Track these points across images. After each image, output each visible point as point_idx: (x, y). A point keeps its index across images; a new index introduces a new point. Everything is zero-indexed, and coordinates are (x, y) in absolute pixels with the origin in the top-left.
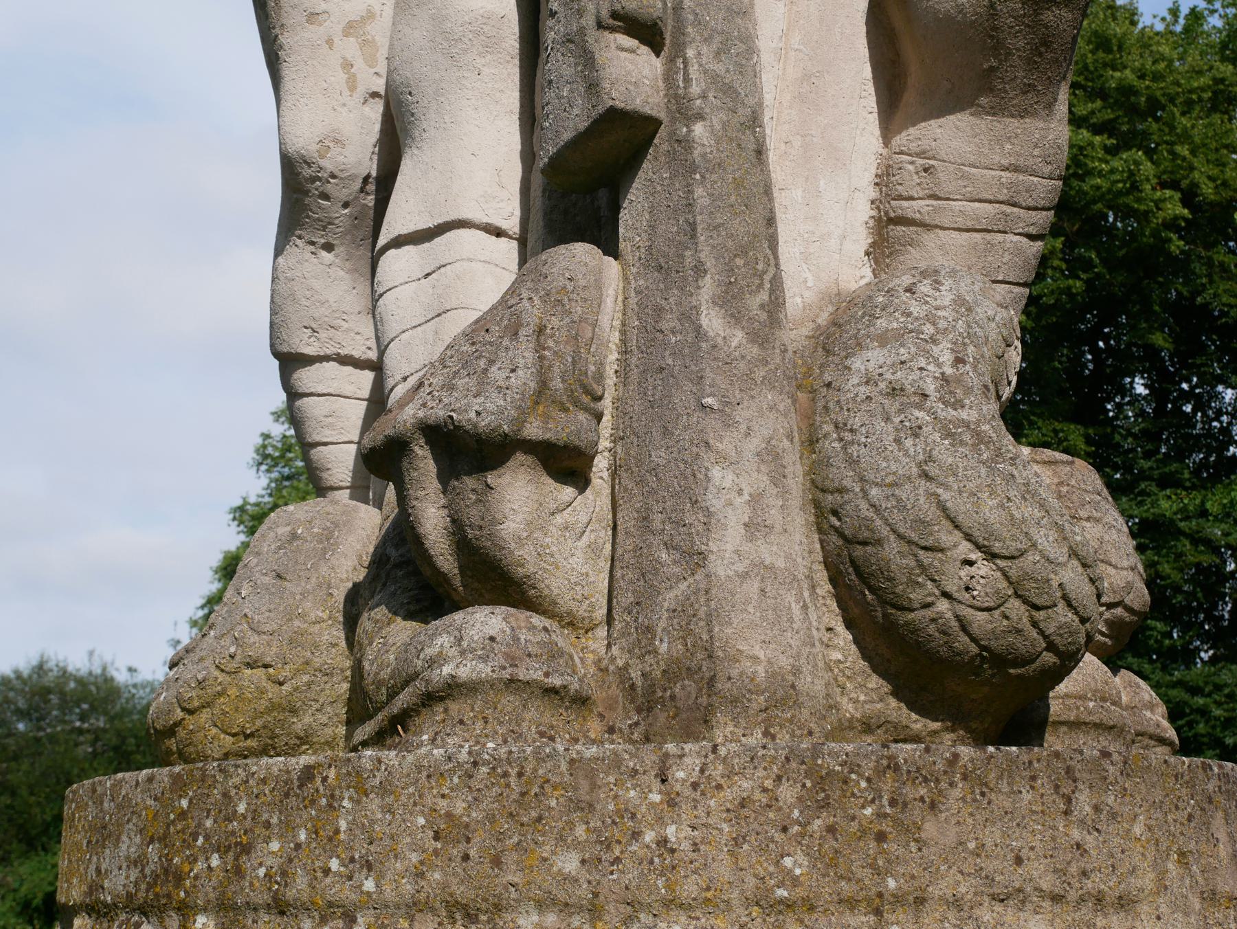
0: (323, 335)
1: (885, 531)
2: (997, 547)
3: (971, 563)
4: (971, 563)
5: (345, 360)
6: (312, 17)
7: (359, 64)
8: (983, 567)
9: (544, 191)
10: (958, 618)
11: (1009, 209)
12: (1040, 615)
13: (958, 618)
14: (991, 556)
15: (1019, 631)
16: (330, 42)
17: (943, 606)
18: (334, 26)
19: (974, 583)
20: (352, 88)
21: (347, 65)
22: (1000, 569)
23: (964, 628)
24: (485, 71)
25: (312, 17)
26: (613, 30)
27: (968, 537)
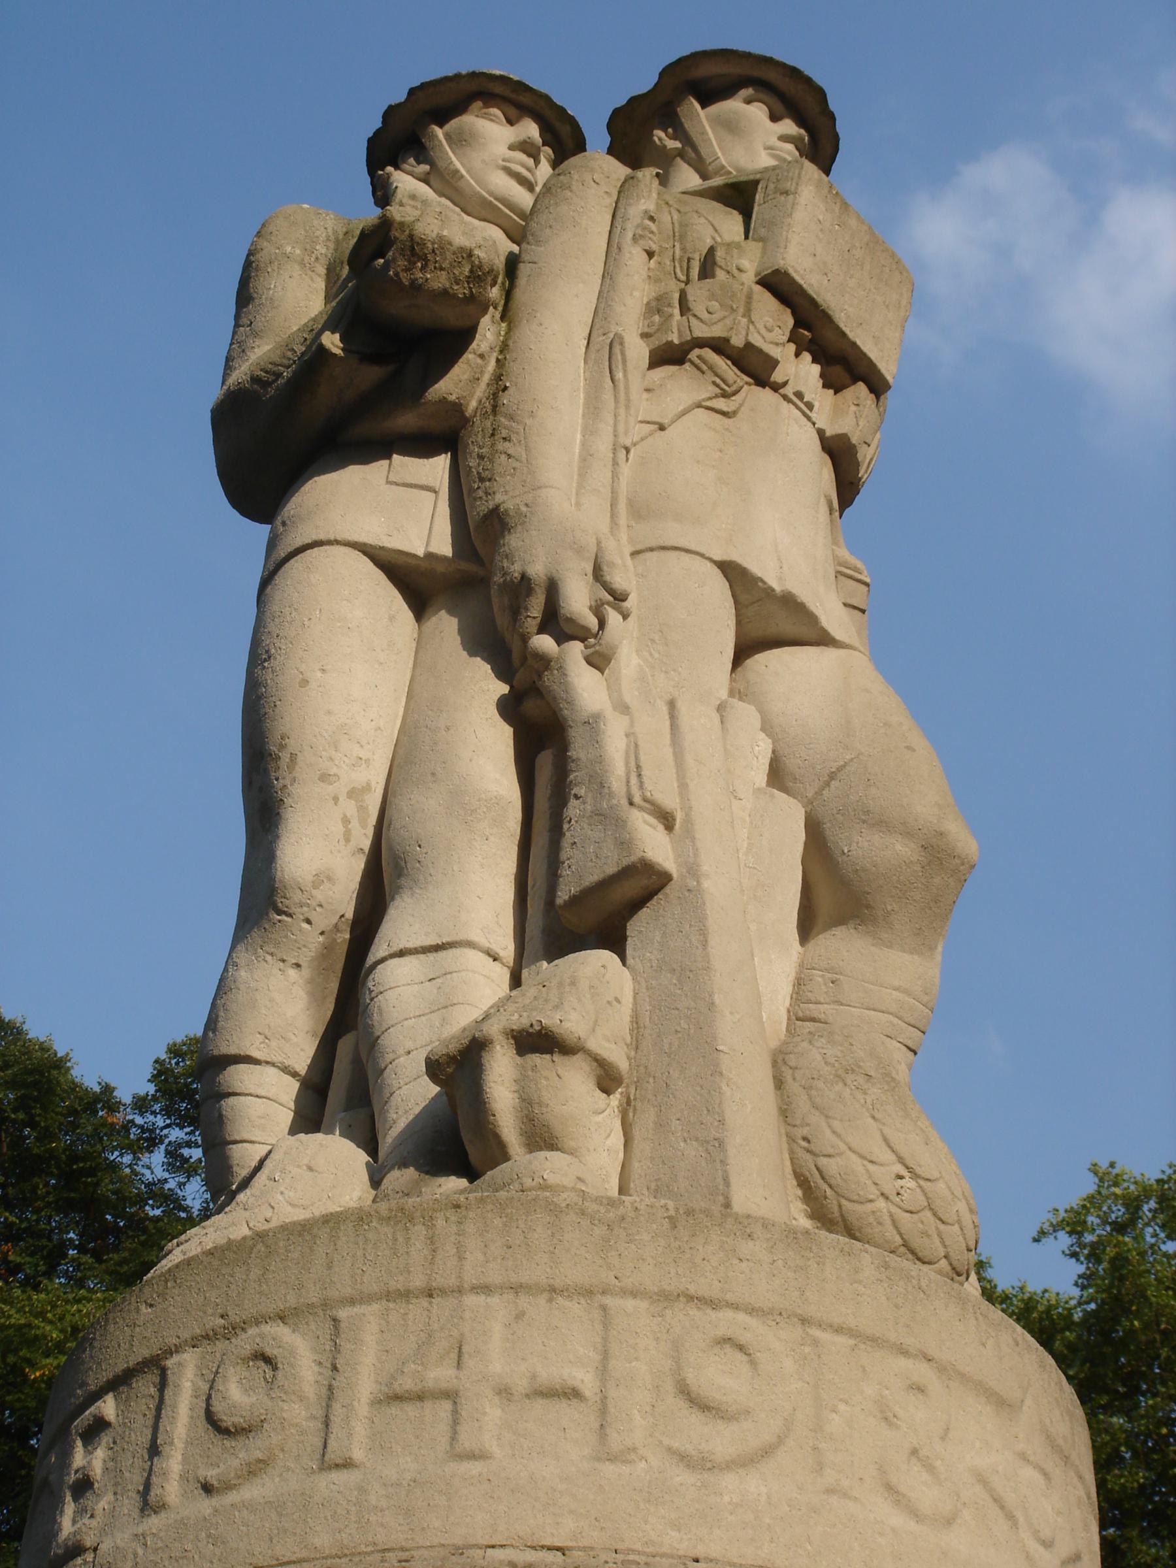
0: (274, 1044)
1: (843, 1147)
2: (918, 1170)
3: (901, 1177)
4: (901, 1177)
5: (286, 1070)
6: (325, 778)
7: (355, 825)
8: (909, 1183)
9: (543, 931)
10: (891, 1215)
11: (896, 1021)
12: (942, 1227)
13: (891, 1215)
14: (915, 1176)
15: (928, 1236)
16: (336, 799)
17: (881, 1204)
18: (341, 788)
19: (902, 1192)
20: (347, 840)
21: (346, 821)
22: (920, 1187)
23: (894, 1223)
24: (492, 839)
25: (325, 778)
26: (641, 808)
27: (901, 1160)
